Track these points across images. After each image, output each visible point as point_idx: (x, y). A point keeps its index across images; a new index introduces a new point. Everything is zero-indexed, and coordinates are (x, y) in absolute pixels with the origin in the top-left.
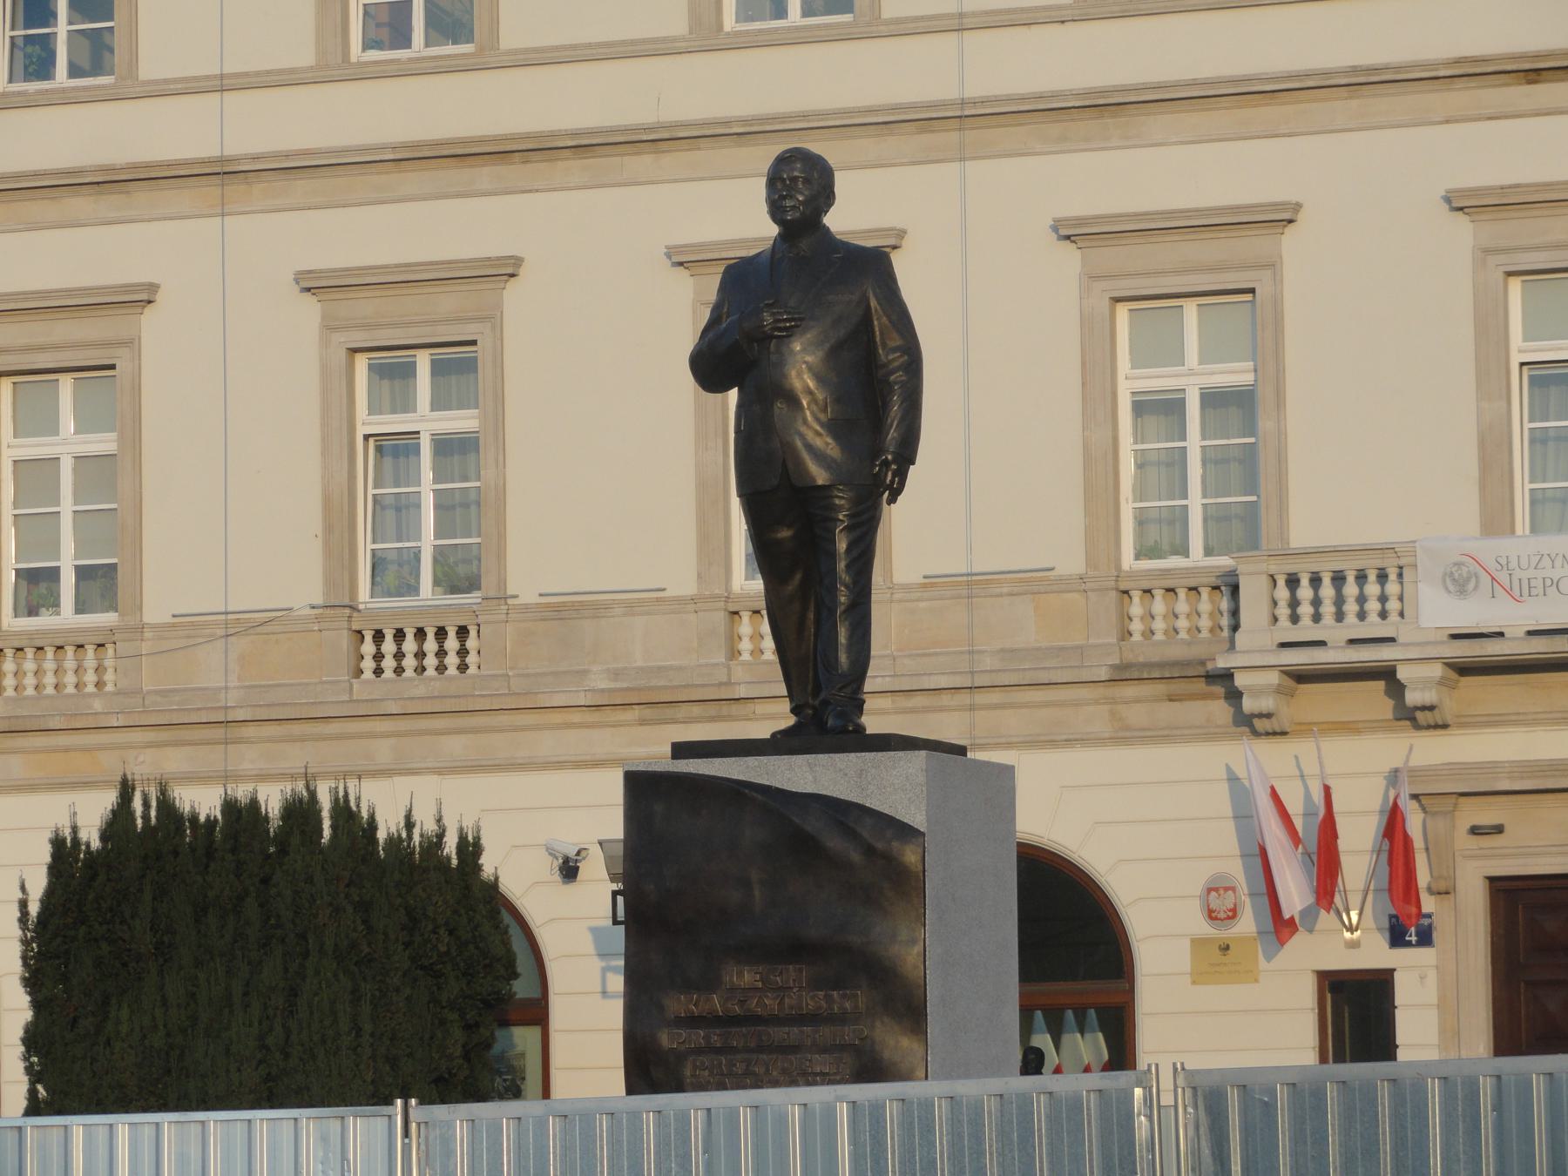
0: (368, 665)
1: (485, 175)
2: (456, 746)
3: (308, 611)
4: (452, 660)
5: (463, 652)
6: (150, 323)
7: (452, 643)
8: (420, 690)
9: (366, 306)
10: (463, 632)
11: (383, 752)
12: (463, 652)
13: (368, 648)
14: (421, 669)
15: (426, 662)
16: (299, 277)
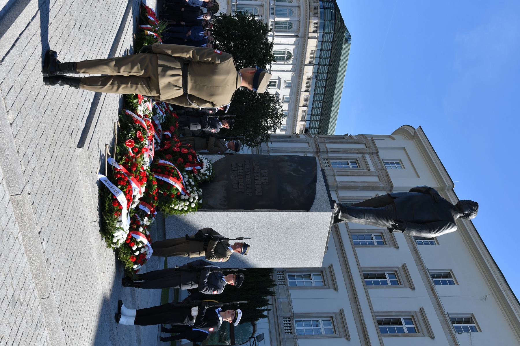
0: (285, 319)
1: (362, 335)
2: (273, 331)
3: (293, 311)
4: (287, 331)
5: (288, 333)
6: (332, 291)
7: (289, 331)
8: (282, 327)
9: (339, 319)
10: (291, 333)
11: (272, 321)
12: (288, 333)
13: (288, 319)
14: (285, 327)
15: (286, 327)
16: (343, 309)
